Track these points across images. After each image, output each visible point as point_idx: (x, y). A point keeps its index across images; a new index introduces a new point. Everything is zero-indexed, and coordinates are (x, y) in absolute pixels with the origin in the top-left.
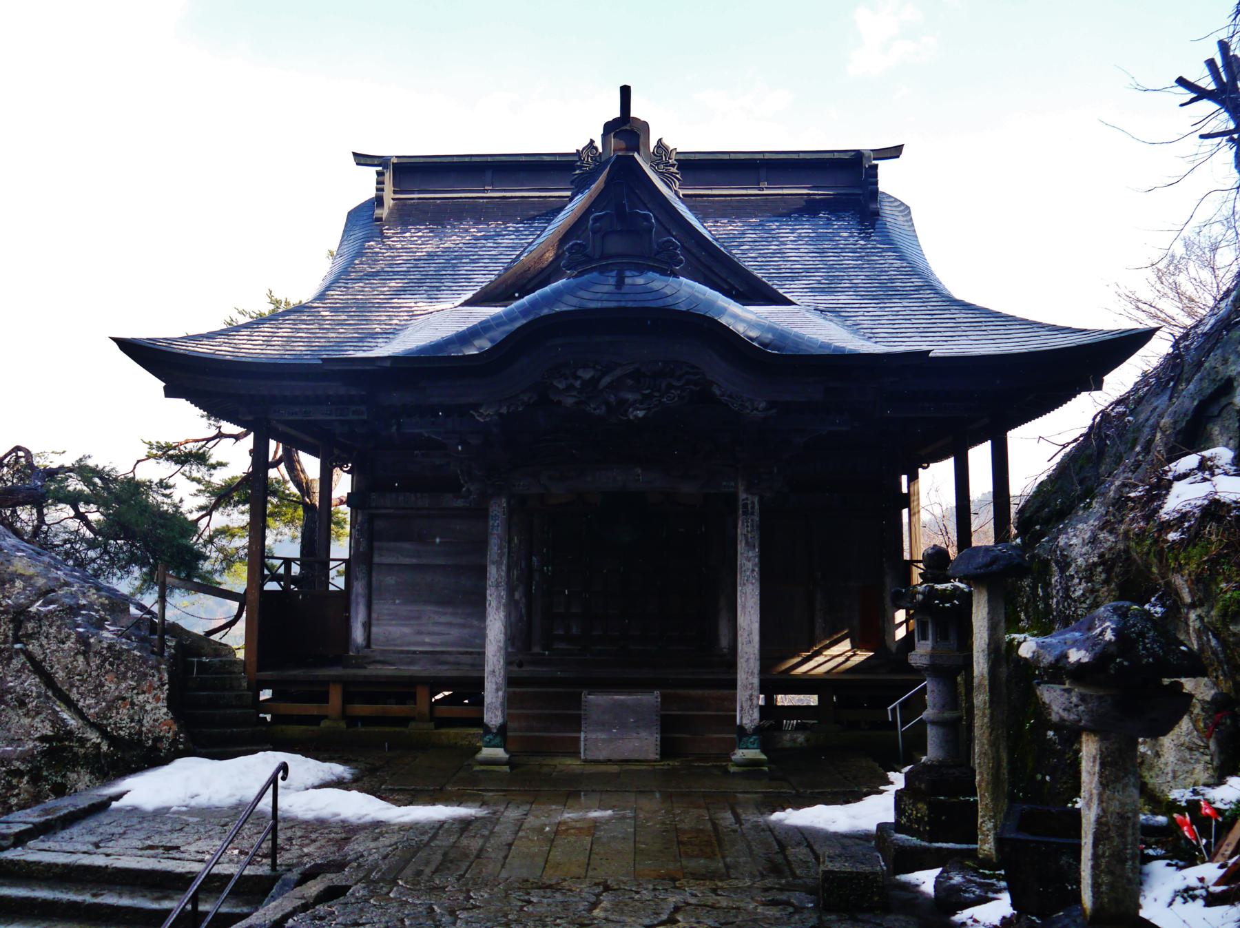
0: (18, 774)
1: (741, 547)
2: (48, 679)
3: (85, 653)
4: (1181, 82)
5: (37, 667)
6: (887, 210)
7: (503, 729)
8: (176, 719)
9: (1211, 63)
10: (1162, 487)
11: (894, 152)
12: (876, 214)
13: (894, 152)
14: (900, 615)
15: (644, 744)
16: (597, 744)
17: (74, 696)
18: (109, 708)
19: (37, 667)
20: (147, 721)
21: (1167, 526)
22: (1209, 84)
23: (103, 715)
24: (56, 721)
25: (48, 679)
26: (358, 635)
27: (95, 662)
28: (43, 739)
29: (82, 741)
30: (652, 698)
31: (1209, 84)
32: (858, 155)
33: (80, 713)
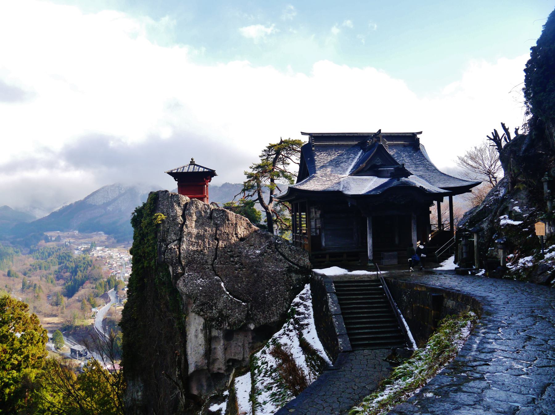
0: (284, 274)
1: (413, 225)
2: (284, 256)
3: (291, 251)
4: (487, 136)
5: (281, 254)
6: (420, 147)
7: (373, 260)
8: (311, 262)
9: (492, 133)
10: (500, 220)
11: (421, 133)
12: (419, 149)
13: (421, 133)
14: (430, 235)
15: (395, 262)
16: (386, 262)
17: (290, 259)
18: (299, 260)
19: (281, 254)
20: (306, 263)
21: (501, 226)
22: (493, 138)
23: (298, 262)
24: (289, 264)
25: (284, 256)
26: (323, 244)
27: (293, 252)
28: (287, 267)
29: (294, 267)
30: (396, 253)
31: (493, 138)
32: (413, 133)
33: (292, 262)
